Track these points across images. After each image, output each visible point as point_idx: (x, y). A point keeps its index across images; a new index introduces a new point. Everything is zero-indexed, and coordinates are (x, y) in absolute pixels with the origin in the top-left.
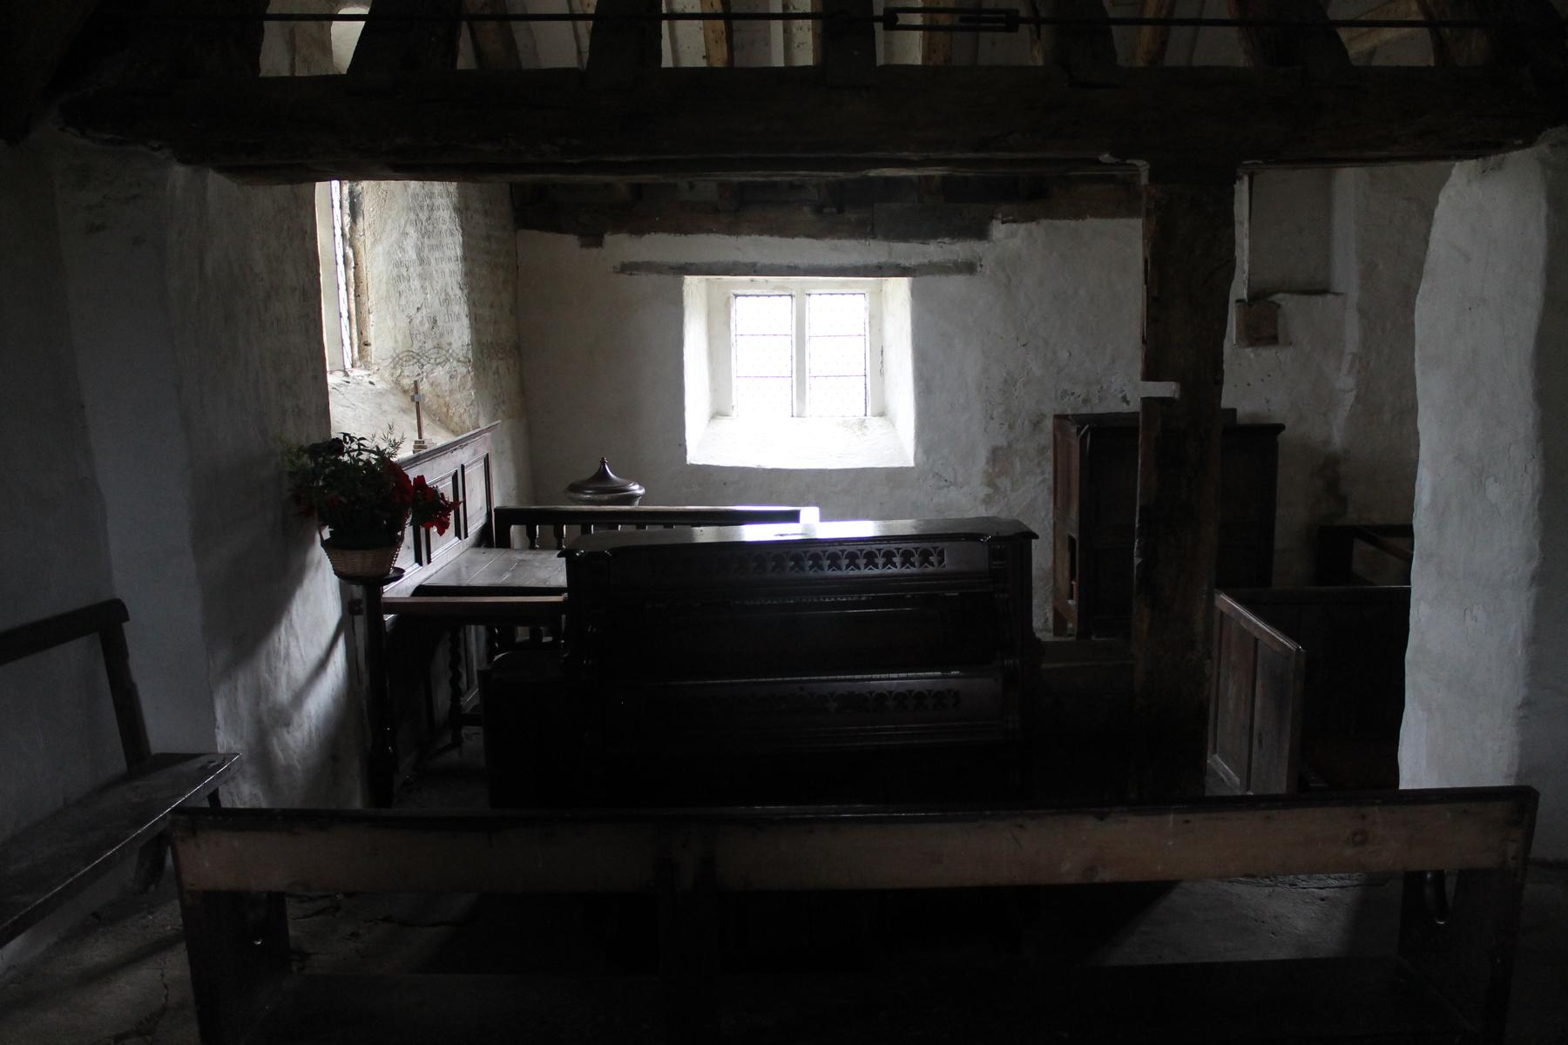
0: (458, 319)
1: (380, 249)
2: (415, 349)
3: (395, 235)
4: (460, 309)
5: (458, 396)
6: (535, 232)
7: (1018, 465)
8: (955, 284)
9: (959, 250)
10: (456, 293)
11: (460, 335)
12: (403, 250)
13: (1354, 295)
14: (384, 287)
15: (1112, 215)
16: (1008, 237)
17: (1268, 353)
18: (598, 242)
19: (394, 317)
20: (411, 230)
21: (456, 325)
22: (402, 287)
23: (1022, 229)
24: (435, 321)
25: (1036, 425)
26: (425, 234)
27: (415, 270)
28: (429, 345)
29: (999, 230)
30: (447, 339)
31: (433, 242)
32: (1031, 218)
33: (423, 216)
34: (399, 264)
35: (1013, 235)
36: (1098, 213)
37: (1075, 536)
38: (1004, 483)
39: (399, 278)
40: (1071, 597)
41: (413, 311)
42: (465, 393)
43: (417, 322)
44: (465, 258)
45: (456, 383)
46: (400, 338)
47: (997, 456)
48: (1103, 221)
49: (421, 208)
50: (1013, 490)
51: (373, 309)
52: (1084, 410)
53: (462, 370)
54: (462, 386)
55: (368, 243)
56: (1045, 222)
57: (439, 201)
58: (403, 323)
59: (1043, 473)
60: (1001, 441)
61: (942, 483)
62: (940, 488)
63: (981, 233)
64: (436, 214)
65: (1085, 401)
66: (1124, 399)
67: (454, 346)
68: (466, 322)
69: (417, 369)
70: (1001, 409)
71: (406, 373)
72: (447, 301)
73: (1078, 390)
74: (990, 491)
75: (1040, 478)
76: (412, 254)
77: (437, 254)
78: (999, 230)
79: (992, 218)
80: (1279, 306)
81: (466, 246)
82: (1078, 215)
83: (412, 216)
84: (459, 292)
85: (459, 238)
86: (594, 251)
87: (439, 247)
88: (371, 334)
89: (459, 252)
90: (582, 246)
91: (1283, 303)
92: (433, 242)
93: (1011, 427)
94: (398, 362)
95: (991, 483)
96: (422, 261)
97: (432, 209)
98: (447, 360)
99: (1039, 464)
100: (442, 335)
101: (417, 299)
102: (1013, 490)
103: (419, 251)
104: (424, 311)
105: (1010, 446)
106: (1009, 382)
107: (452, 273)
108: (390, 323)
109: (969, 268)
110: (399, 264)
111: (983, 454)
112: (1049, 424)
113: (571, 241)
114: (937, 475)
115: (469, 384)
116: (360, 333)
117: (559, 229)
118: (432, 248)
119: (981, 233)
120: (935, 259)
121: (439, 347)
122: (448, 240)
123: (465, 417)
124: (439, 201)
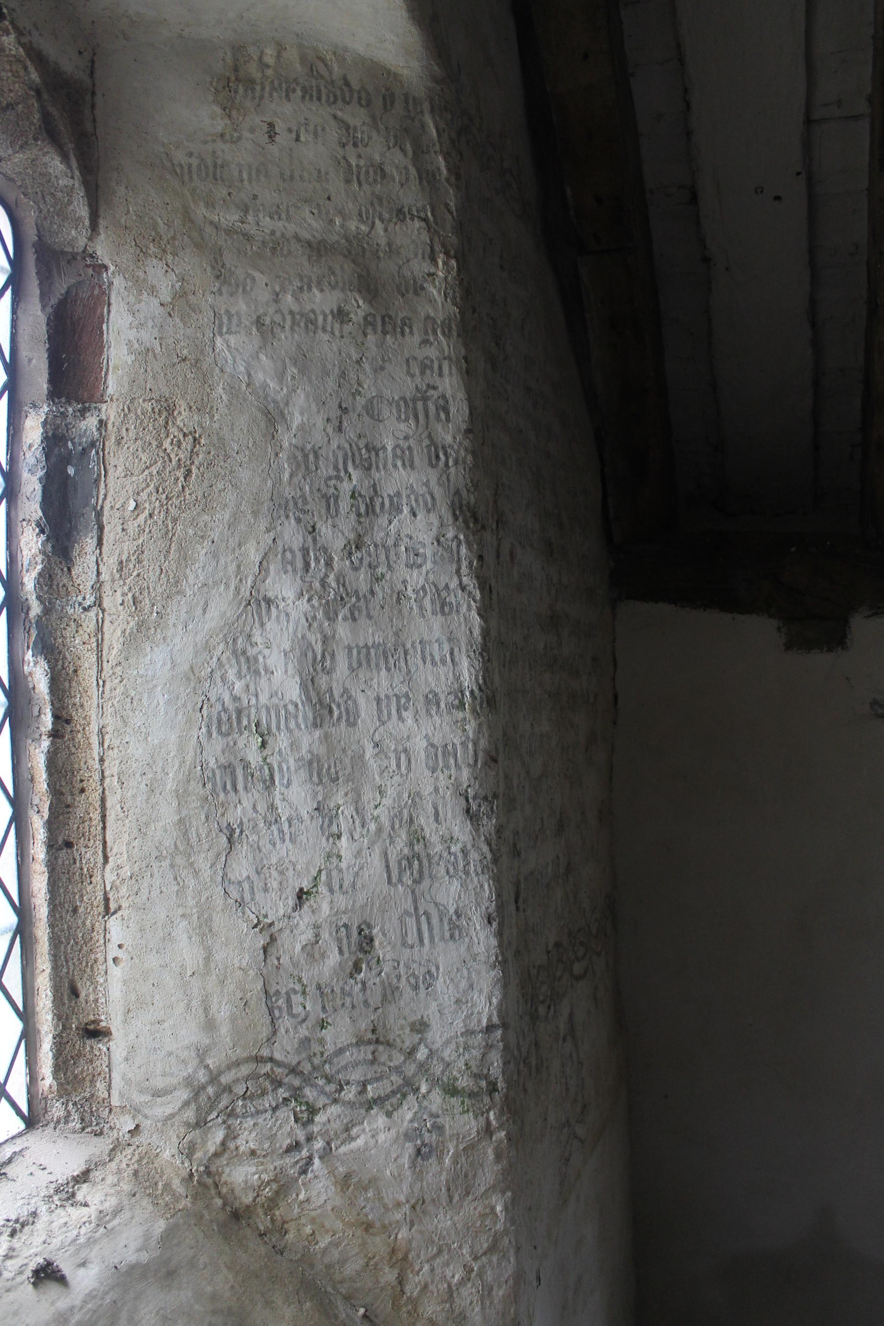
0: (455, 929)
1: (157, 660)
2: (285, 1049)
3: (221, 606)
4: (464, 892)
5: (443, 1221)
6: (665, 609)
10: (451, 830)
11: (458, 990)
12: (251, 665)
14: (167, 813)
18: (836, 639)
19: (204, 928)
20: (284, 587)
21: (446, 956)
22: (244, 807)
24: (366, 942)
26: (338, 601)
27: (295, 743)
28: (340, 1033)
30: (410, 1005)
31: (370, 634)
33: (335, 536)
34: (230, 721)
39: (231, 775)
41: (277, 906)
42: (471, 1209)
43: (293, 944)
44: (488, 699)
45: (438, 1173)
46: (223, 1012)
49: (330, 501)
51: (121, 896)
53: (468, 1124)
54: (461, 1185)
55: (113, 636)
57: (397, 480)
58: (237, 949)
64: (385, 528)
67: (437, 1035)
68: (483, 940)
69: (286, 1127)
71: (247, 1140)
72: (415, 864)
76: (284, 682)
77: (383, 682)
81: (493, 650)
83: (292, 534)
84: (460, 830)
85: (469, 620)
86: (820, 661)
87: (391, 654)
88: (113, 992)
89: (467, 673)
90: (788, 646)
92: (370, 634)
94: (213, 1099)
96: (323, 708)
97: (368, 507)
98: (409, 1087)
100: (390, 993)
101: (301, 856)
103: (314, 667)
104: (324, 905)
107: (438, 755)
108: (187, 952)
110: (230, 721)
113: (760, 632)
115: (489, 1173)
116: (68, 992)
117: (731, 604)
118: (365, 658)
121: (376, 1038)
122: (429, 628)
123: (468, 1295)
124: (397, 480)
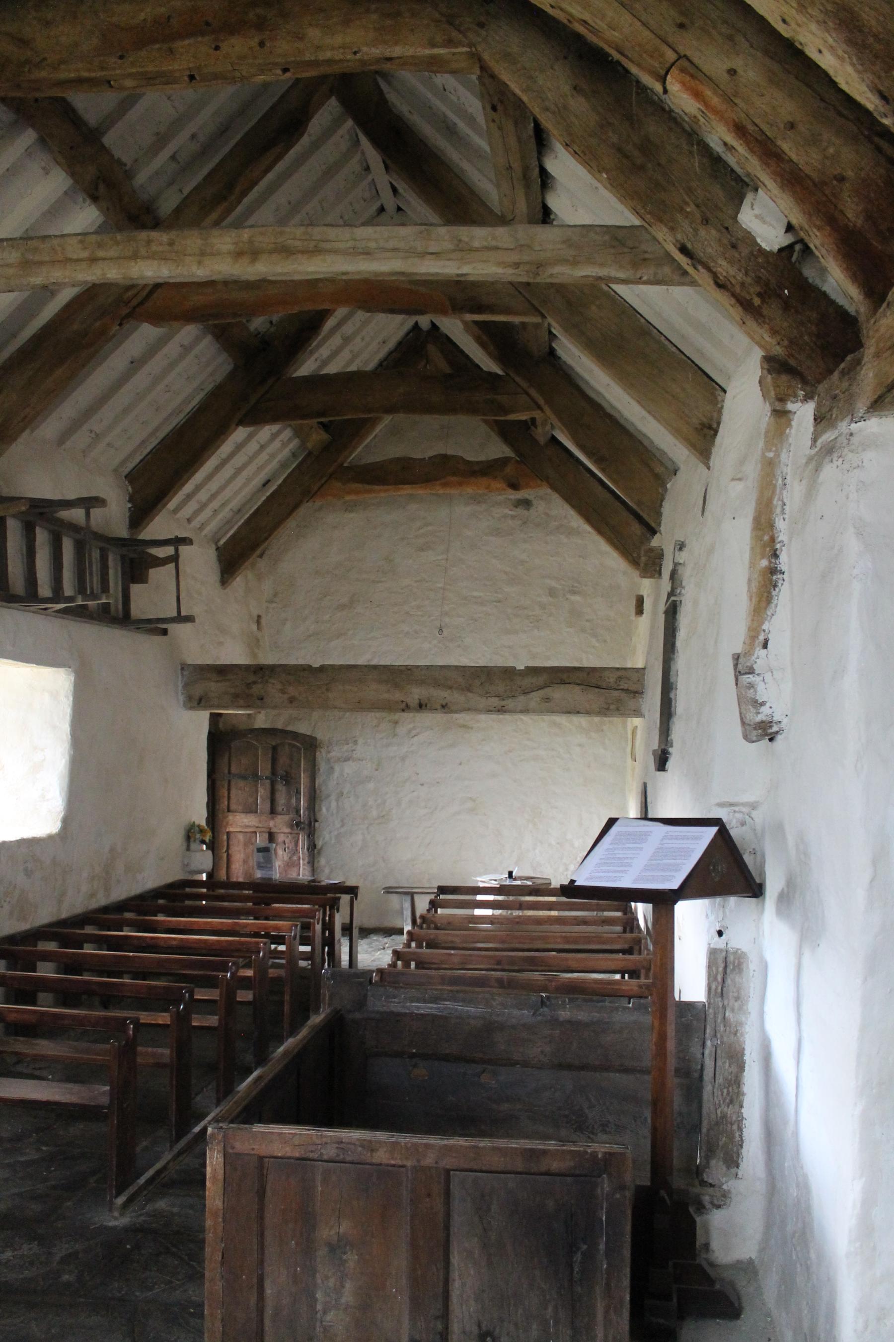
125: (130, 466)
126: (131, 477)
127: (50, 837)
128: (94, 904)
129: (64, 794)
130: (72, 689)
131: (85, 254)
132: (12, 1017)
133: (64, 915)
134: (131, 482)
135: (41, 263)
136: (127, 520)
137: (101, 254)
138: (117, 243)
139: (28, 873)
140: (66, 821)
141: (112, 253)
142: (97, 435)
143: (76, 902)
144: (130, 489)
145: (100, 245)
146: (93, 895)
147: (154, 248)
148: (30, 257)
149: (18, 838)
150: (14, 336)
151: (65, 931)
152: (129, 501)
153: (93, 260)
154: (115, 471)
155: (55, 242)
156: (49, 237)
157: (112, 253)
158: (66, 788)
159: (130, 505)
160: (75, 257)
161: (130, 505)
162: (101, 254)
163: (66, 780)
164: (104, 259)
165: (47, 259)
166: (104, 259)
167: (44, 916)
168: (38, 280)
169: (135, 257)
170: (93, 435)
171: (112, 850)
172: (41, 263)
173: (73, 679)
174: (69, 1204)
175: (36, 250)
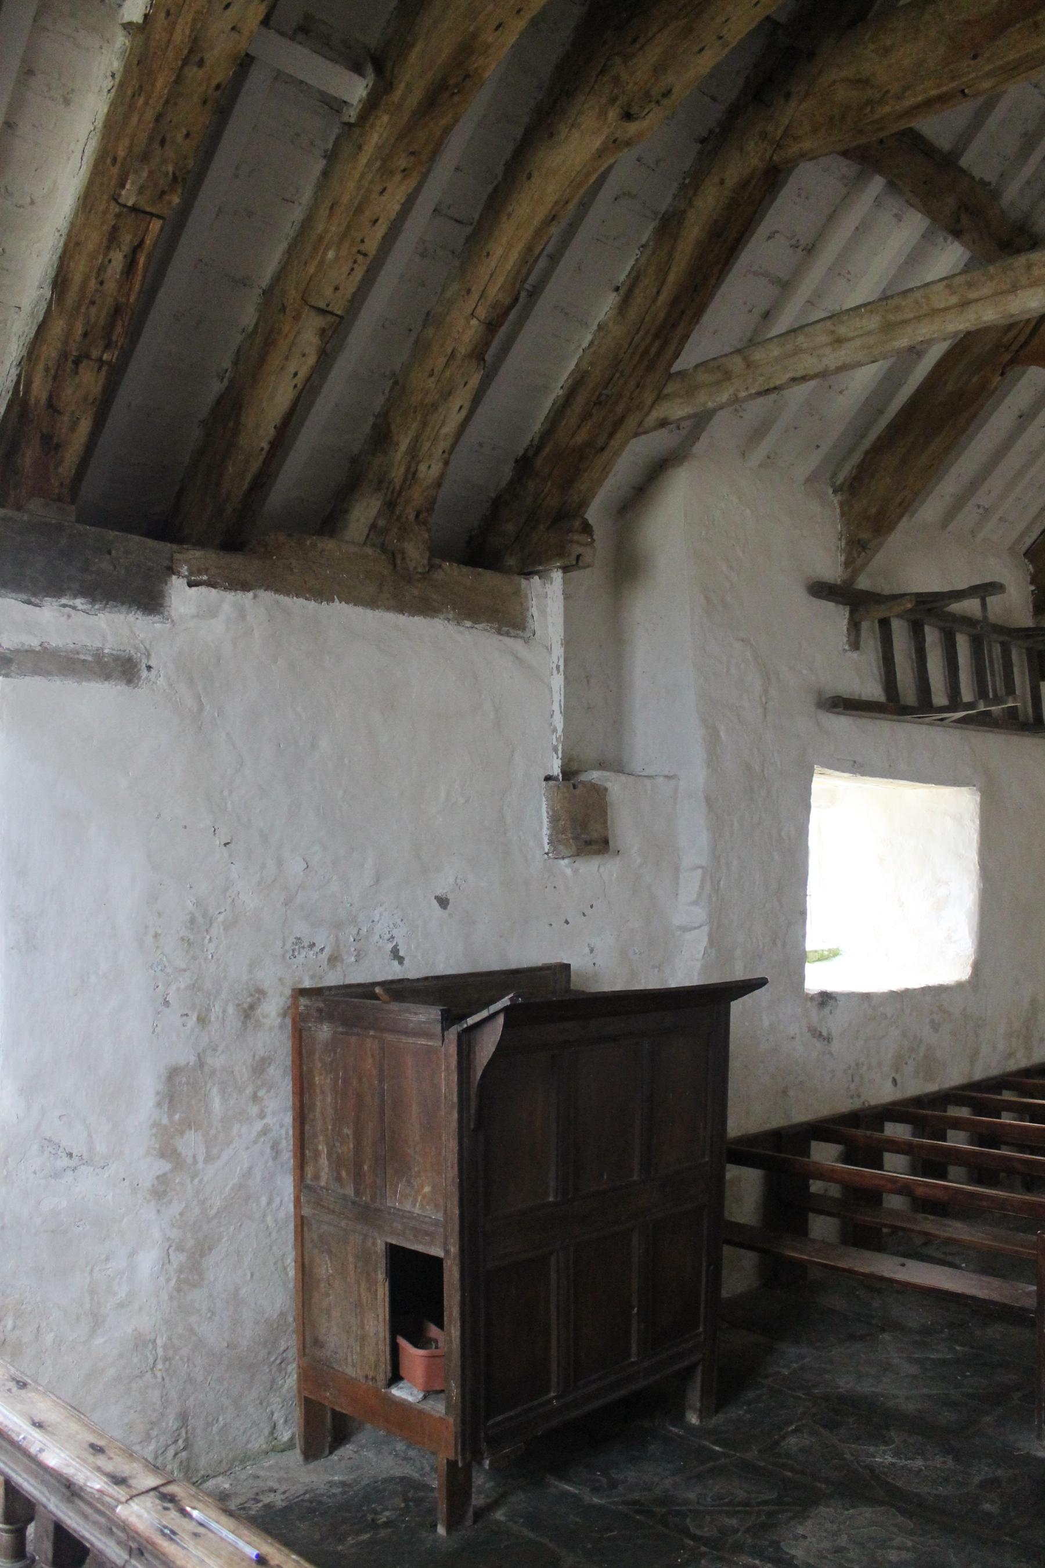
7: (217, 1105)
8: (99, 697)
9: (107, 627)
13: (696, 776)
15: (372, 603)
16: (200, 615)
17: (591, 867)
23: (228, 601)
25: (248, 1012)
29: (183, 597)
32: (244, 586)
35: (212, 613)
36: (353, 598)
37: (441, 1246)
38: (191, 1144)
40: (396, 1377)
47: (180, 1088)
48: (360, 610)
50: (209, 1159)
52: (332, 979)
56: (267, 597)
59: (262, 1115)
60: (186, 1056)
61: (65, 1161)
62: (56, 1175)
63: (149, 599)
65: (334, 960)
66: (395, 954)
70: (184, 981)
73: (323, 938)
74: (165, 1166)
75: (258, 1126)
78: (183, 597)
79: (171, 571)
80: (606, 789)
82: (321, 594)
91: (609, 785)
93: (202, 1020)
95: (167, 1151)
99: (255, 1098)
102: (209, 1159)
105: (201, 1063)
106: (198, 923)
109: (125, 669)
111: (148, 1085)
112: (273, 1009)
114: (50, 1145)
119: (149, 599)
120: (55, 641)
125: (1028, 541)
126: (1031, 554)
127: (960, 985)
128: (1012, 1066)
129: (973, 935)
130: (978, 810)
131: (954, 300)
132: (920, 1191)
133: (978, 1075)
134: (1031, 561)
135: (905, 322)
136: (1031, 606)
137: (972, 295)
138: (992, 278)
139: (935, 1027)
140: (977, 967)
141: (986, 291)
142: (986, 510)
143: (989, 1064)
144: (1030, 567)
145: (970, 285)
146: (1011, 1055)
147: (1036, 272)
148: (892, 317)
149: (923, 985)
150: (881, 412)
151: (979, 1095)
152: (1031, 583)
153: (964, 304)
154: (1011, 549)
155: (918, 294)
156: (911, 290)
157: (986, 291)
158: (975, 929)
159: (1033, 588)
160: (942, 306)
161: (1033, 588)
162: (972, 295)
163: (976, 919)
164: (977, 300)
165: (911, 315)
166: (977, 300)
167: (954, 1076)
168: (903, 342)
169: (1014, 289)
170: (981, 511)
171: (1033, 1001)
172: (905, 322)
173: (978, 799)
174: (988, 1419)
175: (898, 308)
